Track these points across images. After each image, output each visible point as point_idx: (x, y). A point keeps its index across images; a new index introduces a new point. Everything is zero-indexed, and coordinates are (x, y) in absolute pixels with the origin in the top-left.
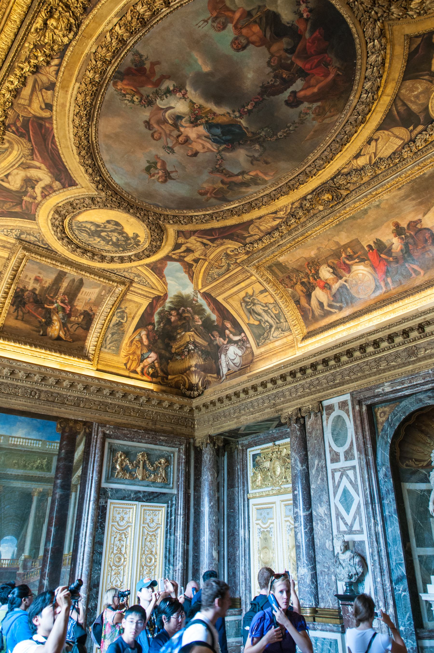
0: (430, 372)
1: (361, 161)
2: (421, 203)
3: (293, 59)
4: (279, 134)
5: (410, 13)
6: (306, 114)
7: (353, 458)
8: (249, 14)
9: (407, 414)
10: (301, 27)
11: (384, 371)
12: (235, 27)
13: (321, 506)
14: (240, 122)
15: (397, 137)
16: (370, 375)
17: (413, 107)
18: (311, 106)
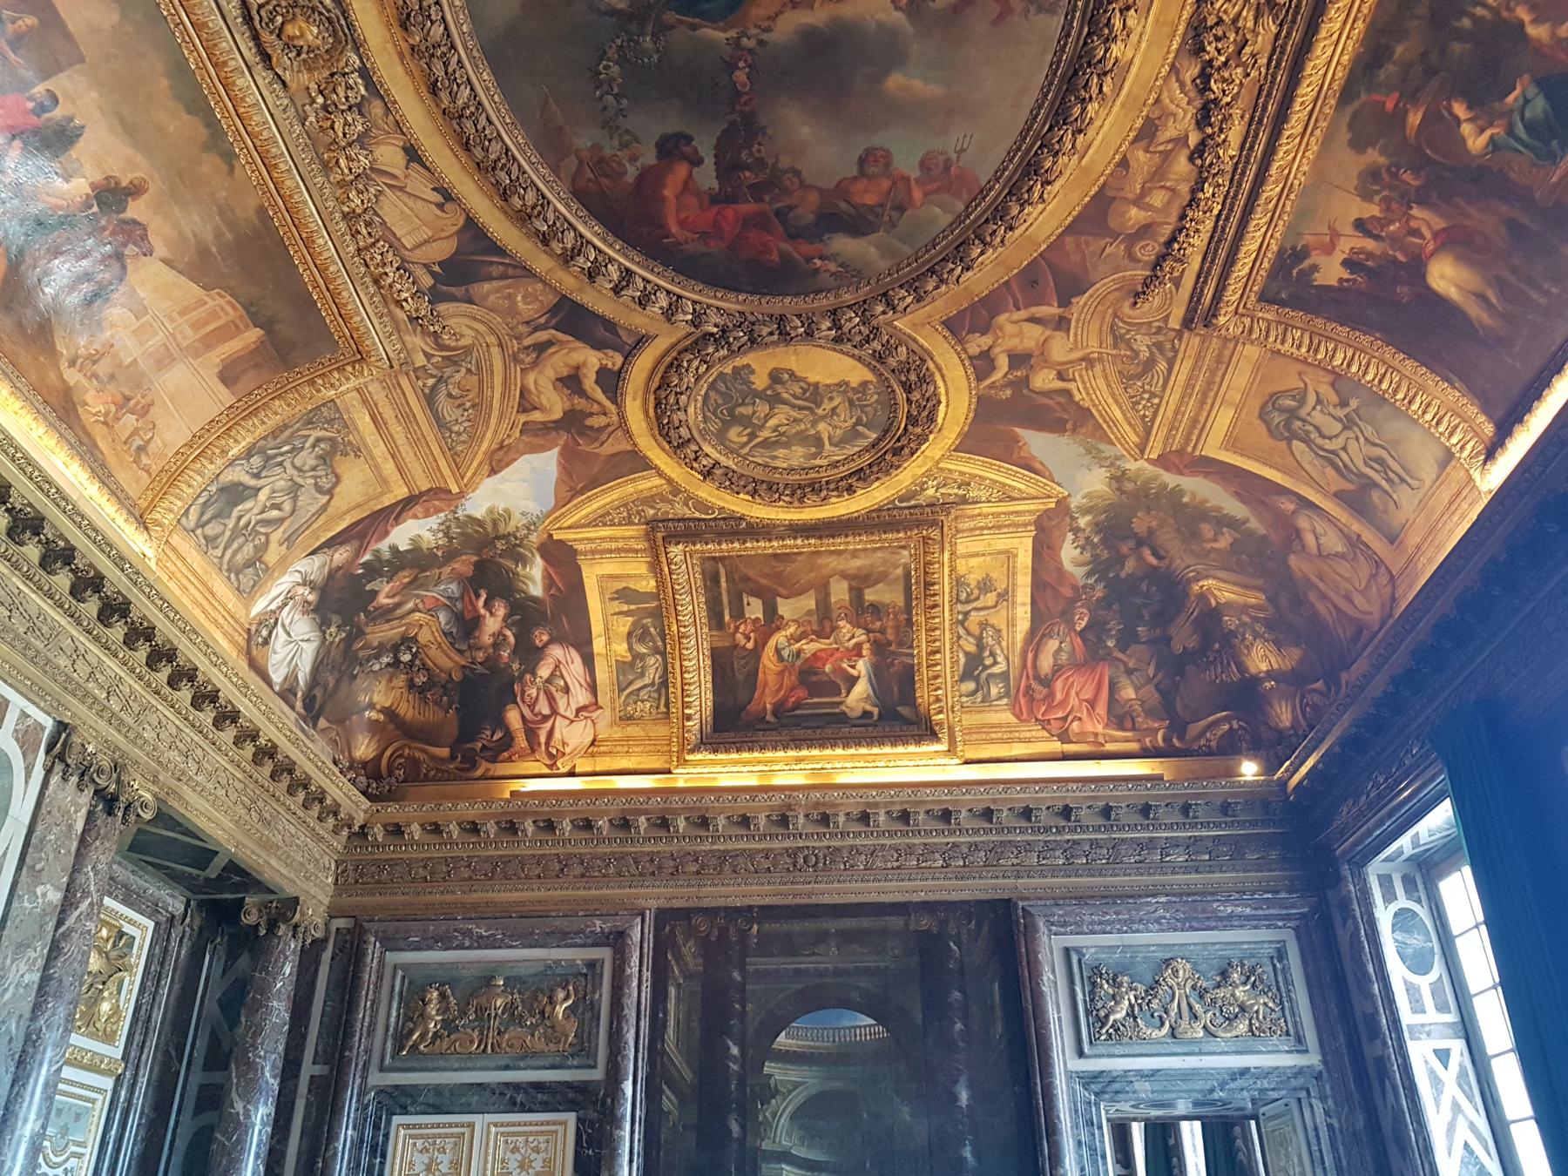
1: (389, 155)
2: (203, 252)
3: (766, 206)
4: (615, 69)
5: (696, 363)
6: (623, 146)
8: (901, 209)
10: (806, 248)
12: (907, 179)
14: (724, 30)
15: (426, 242)
17: (487, 286)
18: (638, 164)
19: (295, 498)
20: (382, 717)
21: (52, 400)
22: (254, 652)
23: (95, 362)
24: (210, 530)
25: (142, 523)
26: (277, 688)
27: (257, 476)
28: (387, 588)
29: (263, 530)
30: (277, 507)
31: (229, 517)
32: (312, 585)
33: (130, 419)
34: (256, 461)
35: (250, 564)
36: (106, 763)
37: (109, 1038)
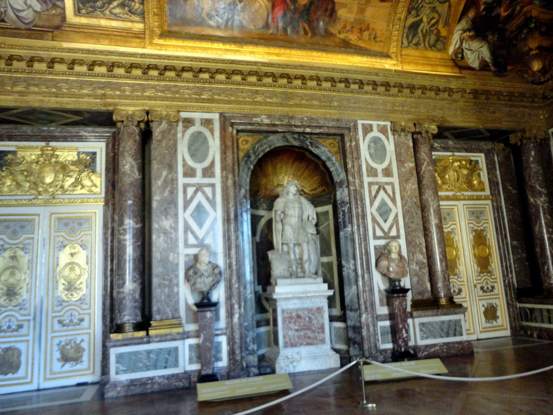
0: (305, 119)
7: (212, 175)
9: (272, 148)
11: (261, 103)
13: (166, 219)
16: (245, 103)
19: (437, 12)
20: (537, 51)
21: (342, 45)
22: (459, 64)
23: (345, 28)
24: (414, 41)
25: (387, 56)
26: (478, 69)
27: (418, 16)
28: (502, 10)
29: (434, 28)
30: (433, 18)
31: (418, 33)
32: (469, 30)
33: (366, 34)
34: (413, 12)
35: (437, 41)
36: (411, 125)
37: (483, 190)
